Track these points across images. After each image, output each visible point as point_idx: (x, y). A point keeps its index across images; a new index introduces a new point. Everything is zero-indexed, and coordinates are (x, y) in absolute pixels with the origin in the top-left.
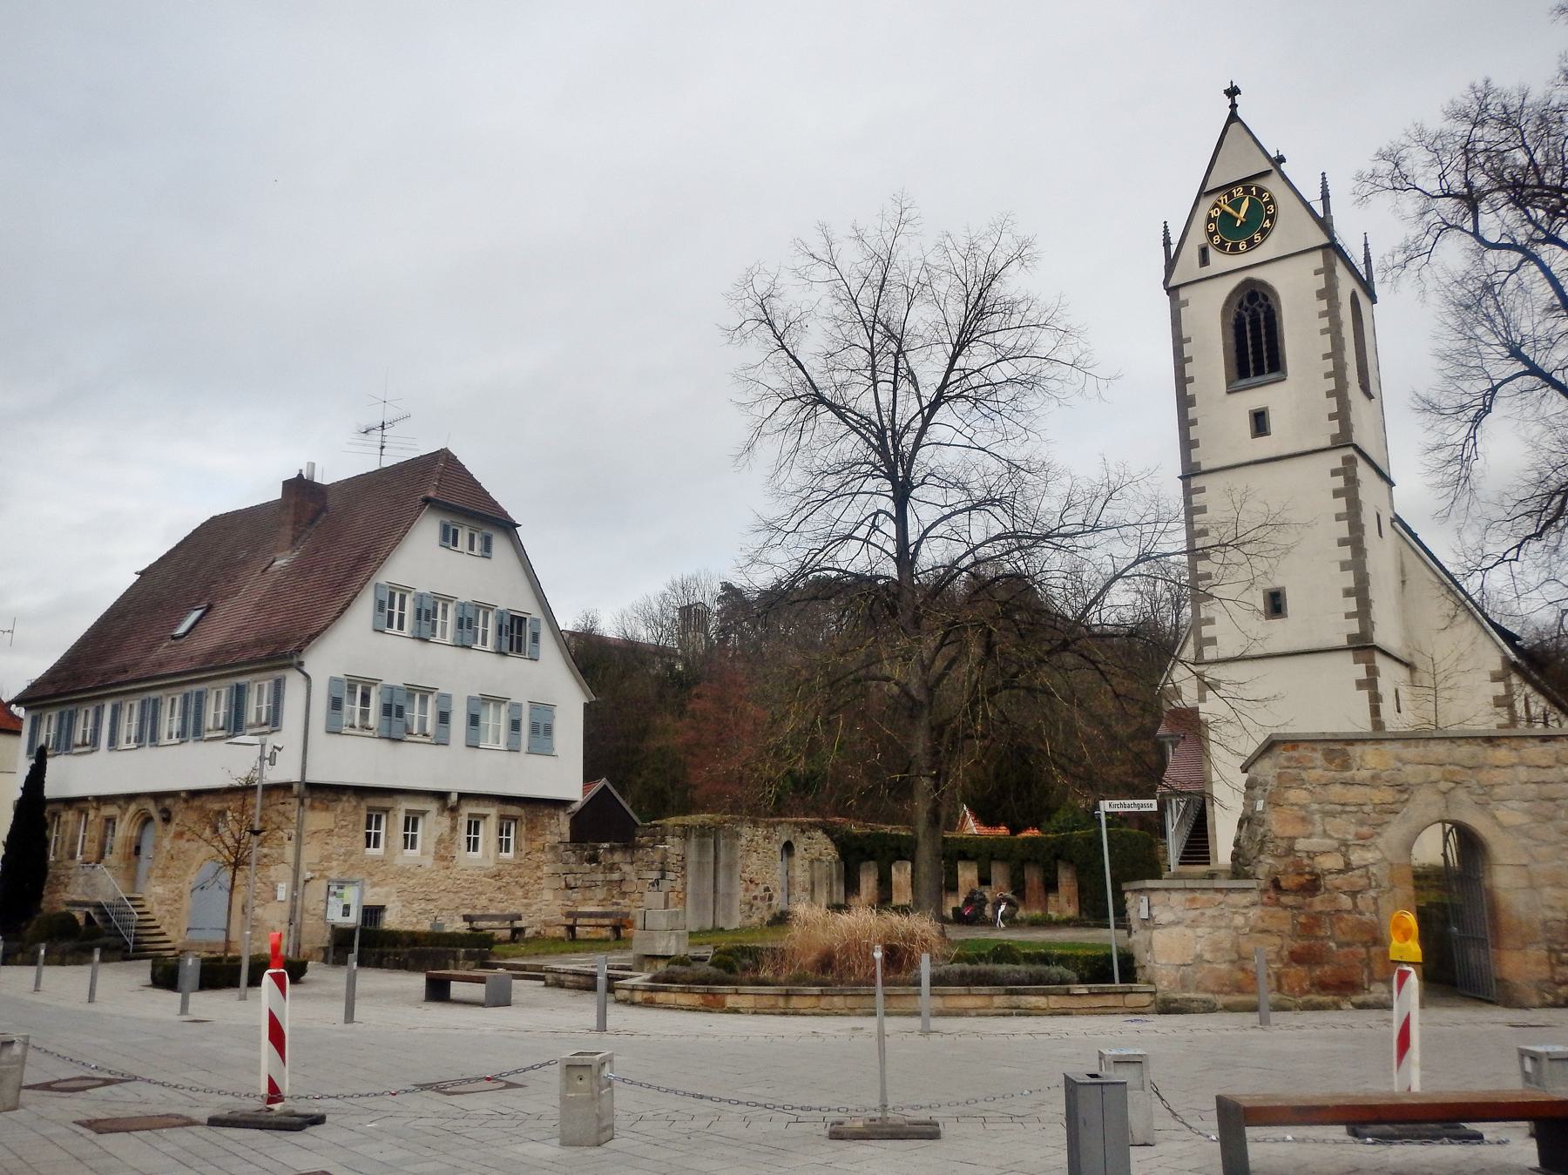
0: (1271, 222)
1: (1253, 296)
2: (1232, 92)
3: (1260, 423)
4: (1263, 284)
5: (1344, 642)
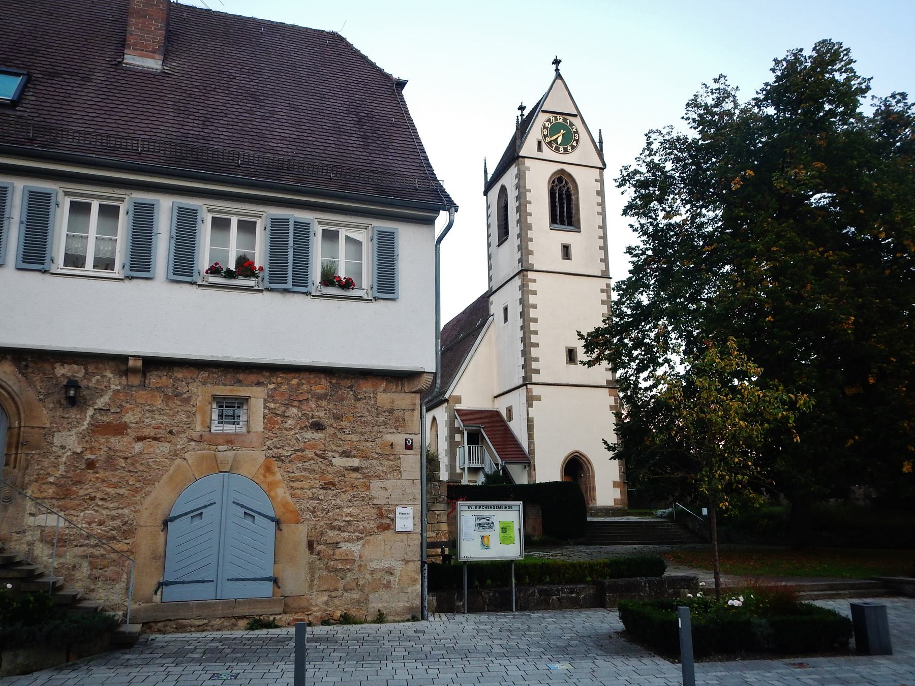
0: (577, 143)
1: (560, 180)
2: (557, 62)
3: (566, 251)
4: (570, 176)
5: (605, 384)
